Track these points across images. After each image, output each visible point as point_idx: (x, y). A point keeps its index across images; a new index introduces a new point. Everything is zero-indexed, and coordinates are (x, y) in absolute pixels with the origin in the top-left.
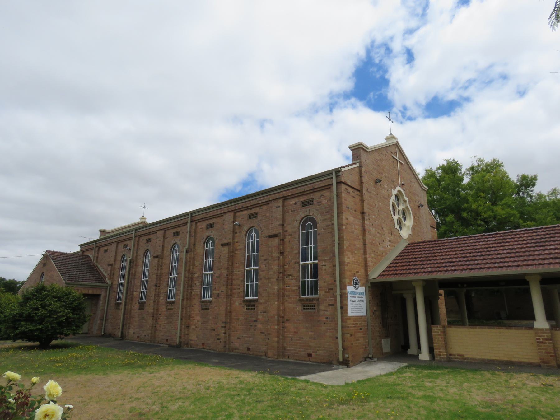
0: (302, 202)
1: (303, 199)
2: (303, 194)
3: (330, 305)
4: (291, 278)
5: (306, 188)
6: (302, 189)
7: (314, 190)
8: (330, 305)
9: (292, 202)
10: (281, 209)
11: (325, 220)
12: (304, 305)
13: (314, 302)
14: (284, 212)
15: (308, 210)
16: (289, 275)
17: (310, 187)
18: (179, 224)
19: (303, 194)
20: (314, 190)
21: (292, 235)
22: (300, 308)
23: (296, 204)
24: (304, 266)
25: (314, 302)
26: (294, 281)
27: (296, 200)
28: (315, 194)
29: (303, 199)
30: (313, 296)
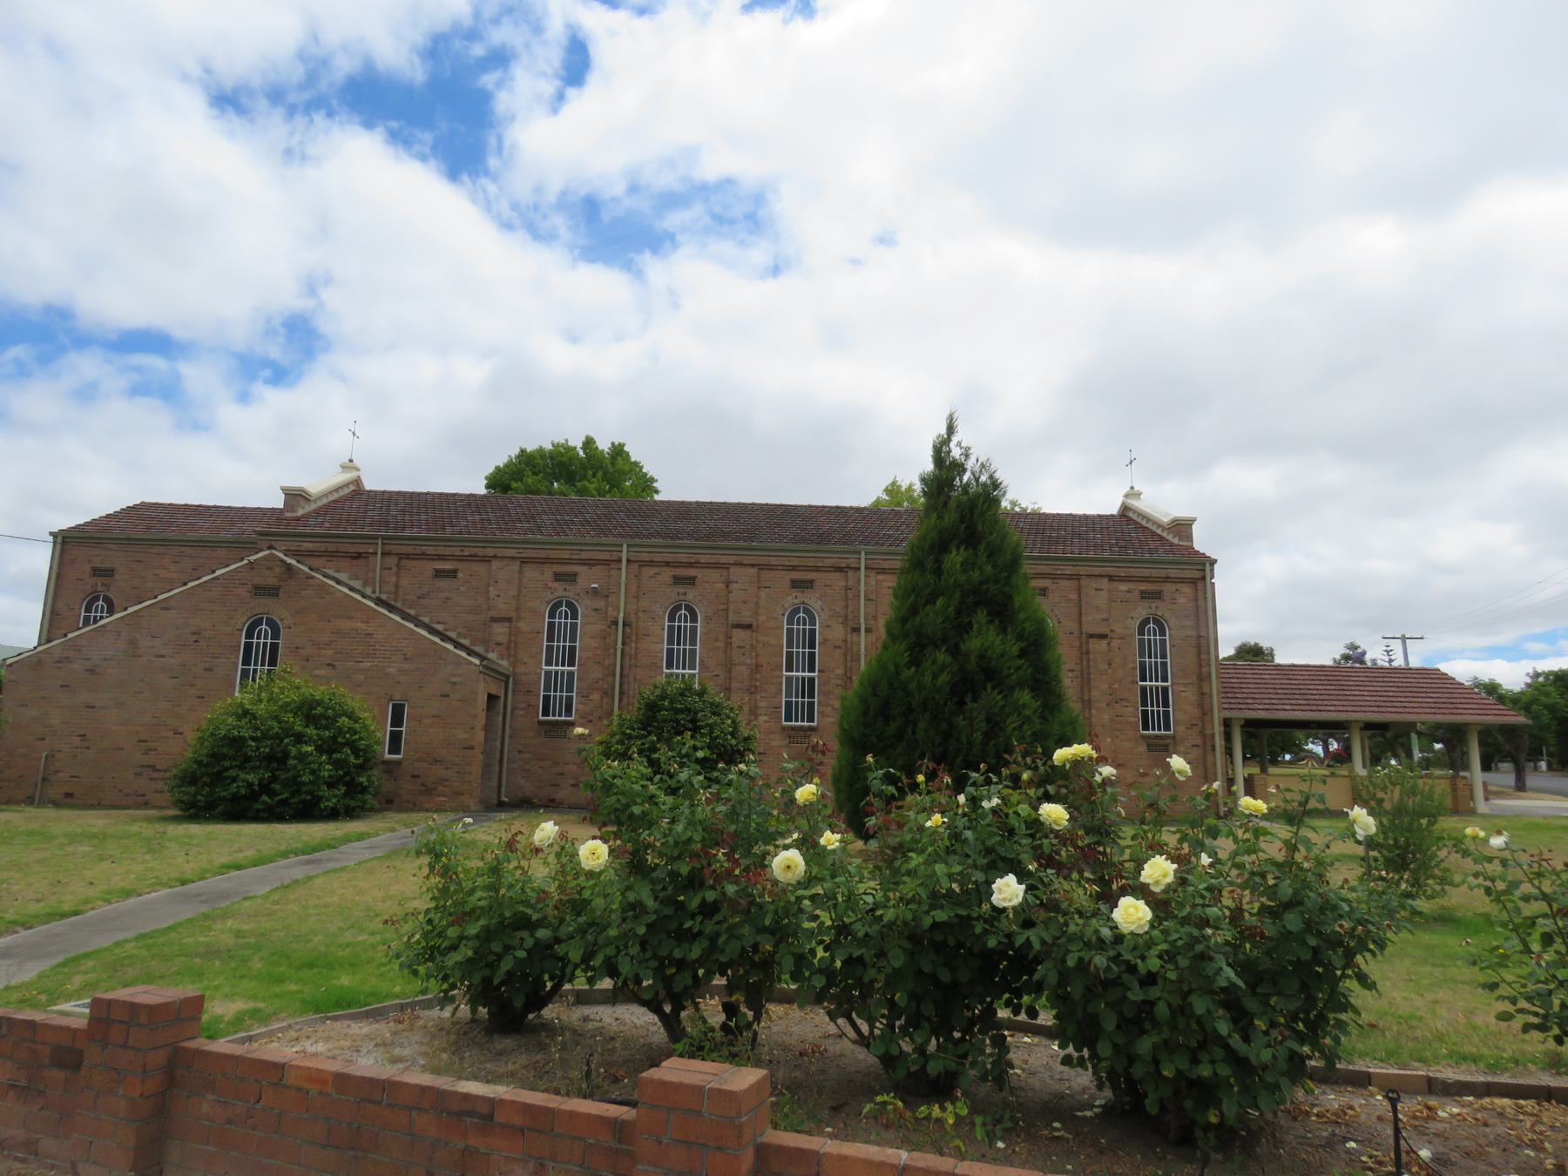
0: (1142, 592)
1: (1144, 587)
2: (1147, 580)
3: (1194, 746)
4: (1124, 703)
5: (1155, 573)
6: (1146, 573)
7: (1167, 579)
8: (1194, 746)
9: (1124, 587)
10: (1104, 594)
11: (1184, 627)
12: (1148, 745)
13: (1168, 741)
14: (1111, 600)
15: (1153, 605)
16: (1121, 699)
17: (1163, 573)
18: (820, 565)
19: (1147, 580)
20: (1167, 579)
21: (1123, 638)
22: (1143, 748)
23: (1129, 592)
24: (789, 679)
25: (1168, 741)
26: (1130, 709)
27: (1131, 586)
28: (1167, 584)
29: (1144, 587)
30: (1163, 732)
